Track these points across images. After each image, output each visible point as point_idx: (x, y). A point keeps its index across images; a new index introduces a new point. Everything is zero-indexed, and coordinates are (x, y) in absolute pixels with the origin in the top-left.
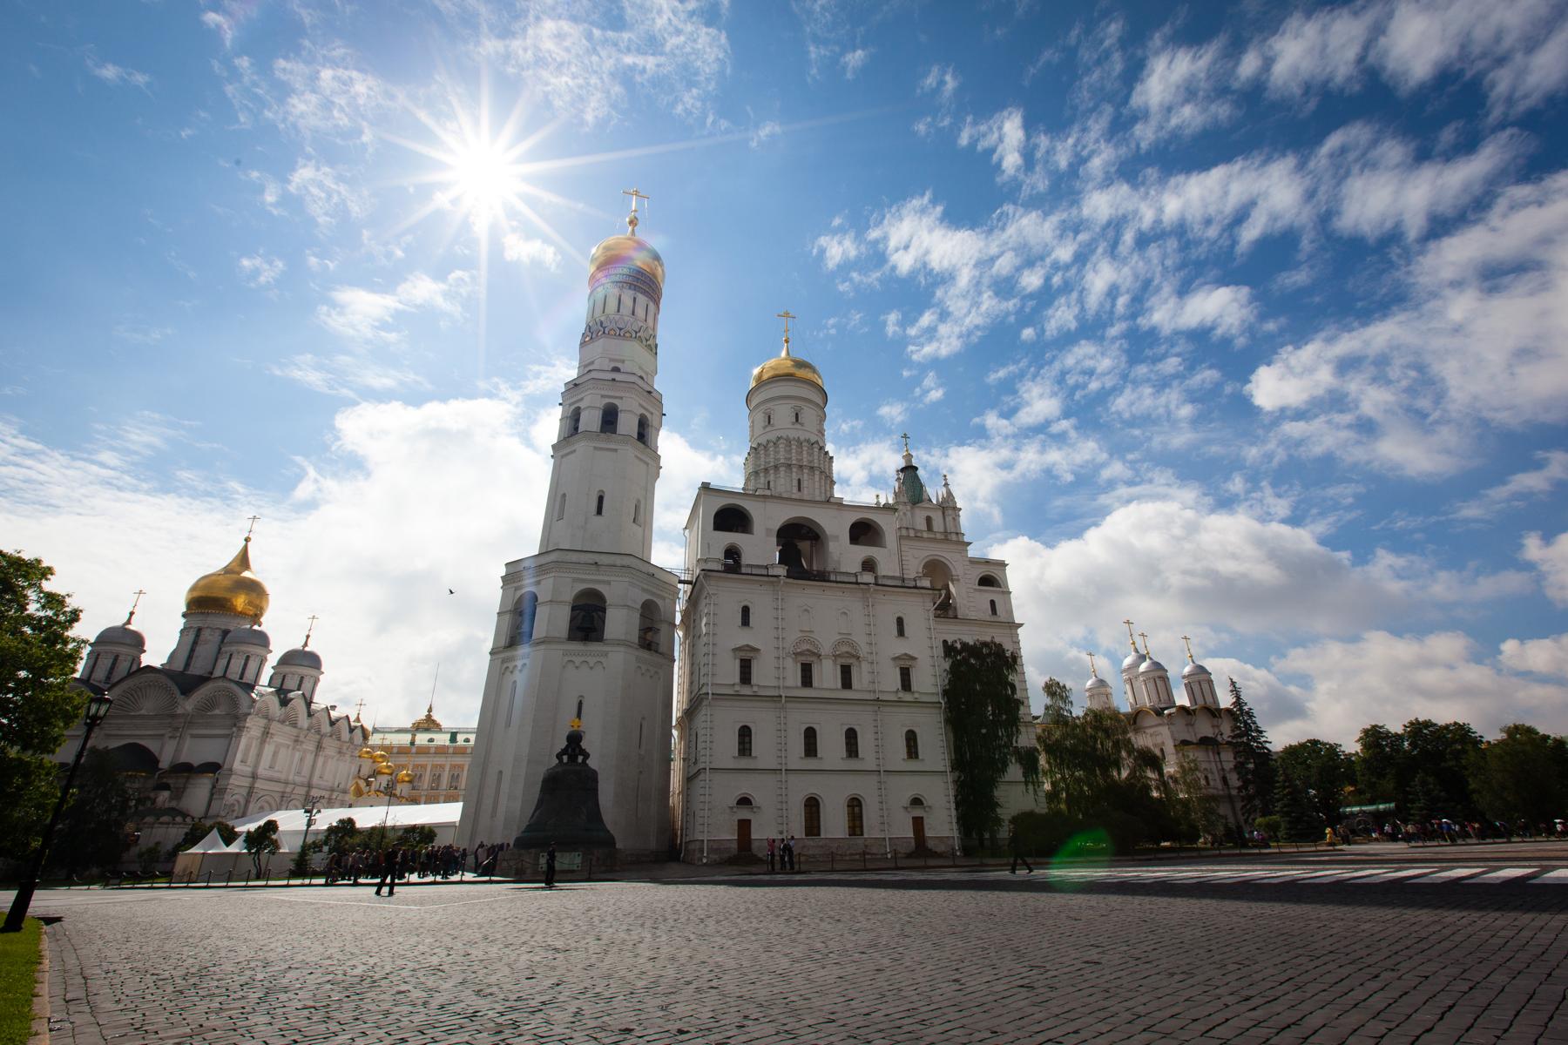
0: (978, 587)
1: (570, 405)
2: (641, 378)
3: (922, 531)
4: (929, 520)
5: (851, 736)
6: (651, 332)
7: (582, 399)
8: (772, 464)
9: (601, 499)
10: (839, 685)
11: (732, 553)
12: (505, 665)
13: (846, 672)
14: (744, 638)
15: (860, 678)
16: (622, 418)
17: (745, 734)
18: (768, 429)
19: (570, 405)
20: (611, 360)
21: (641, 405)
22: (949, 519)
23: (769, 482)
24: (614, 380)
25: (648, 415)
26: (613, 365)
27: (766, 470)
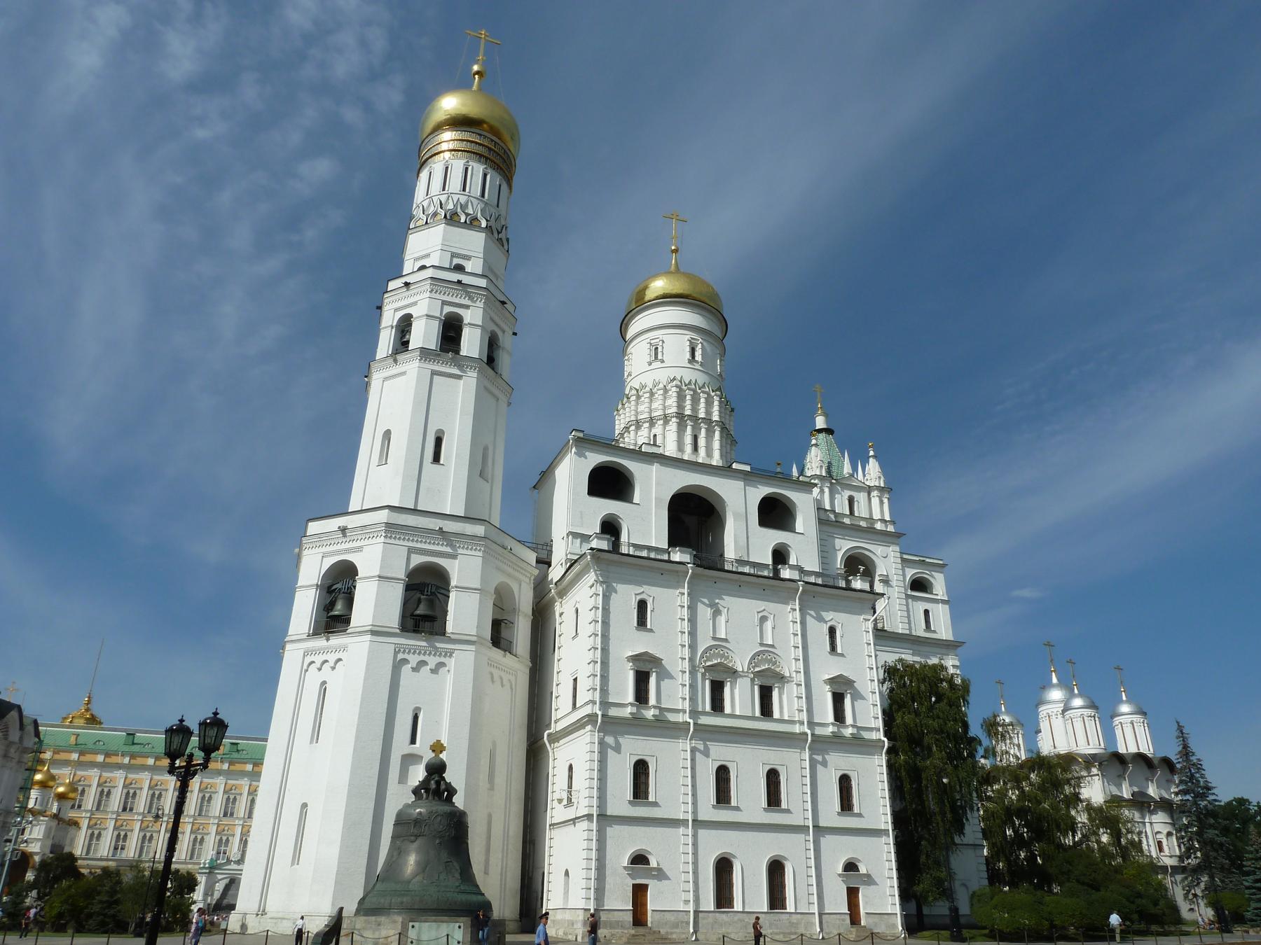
0: (909, 592)
1: (396, 310)
3: (844, 515)
4: (851, 500)
7: (415, 304)
8: (660, 413)
9: (439, 442)
10: (758, 713)
11: (610, 528)
12: (308, 660)
13: (766, 695)
14: (641, 644)
15: (787, 704)
16: (466, 332)
17: (641, 769)
18: (657, 364)
19: (396, 310)
20: (454, 255)
21: (492, 319)
23: (655, 436)
24: (459, 282)
25: (500, 334)
26: (456, 261)
27: (652, 422)
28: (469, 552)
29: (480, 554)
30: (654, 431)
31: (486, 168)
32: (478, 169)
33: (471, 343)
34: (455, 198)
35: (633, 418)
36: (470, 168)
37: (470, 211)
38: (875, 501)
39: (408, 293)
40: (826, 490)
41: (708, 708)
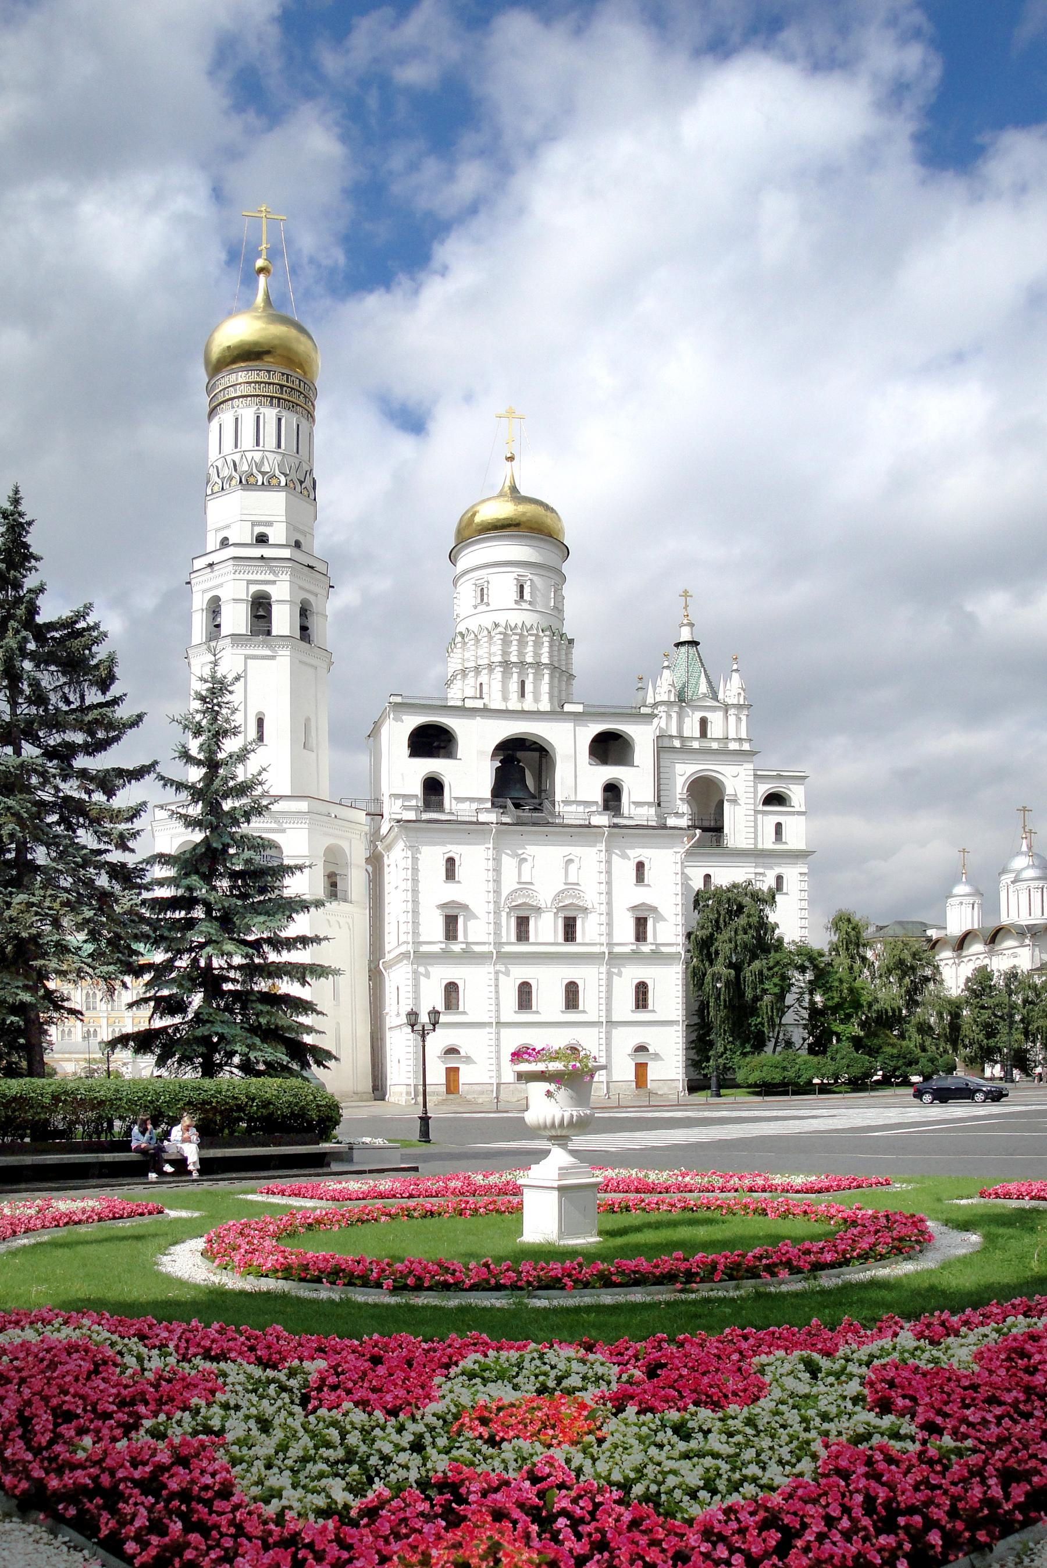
2: (298, 545)
4: (704, 722)
5: (572, 994)
6: (306, 467)
7: (221, 585)
9: (260, 722)
10: (561, 938)
11: (433, 787)
15: (588, 930)
16: (275, 608)
20: (254, 524)
21: (301, 588)
22: (732, 719)
24: (262, 558)
25: (311, 598)
26: (258, 530)
27: (477, 669)
28: (295, 826)
29: (306, 826)
30: (480, 680)
31: (280, 412)
32: (270, 414)
33: (283, 621)
34: (249, 455)
35: (460, 667)
36: (261, 417)
37: (266, 468)
38: (732, 719)
39: (216, 573)
40: (674, 715)
41: (513, 938)
